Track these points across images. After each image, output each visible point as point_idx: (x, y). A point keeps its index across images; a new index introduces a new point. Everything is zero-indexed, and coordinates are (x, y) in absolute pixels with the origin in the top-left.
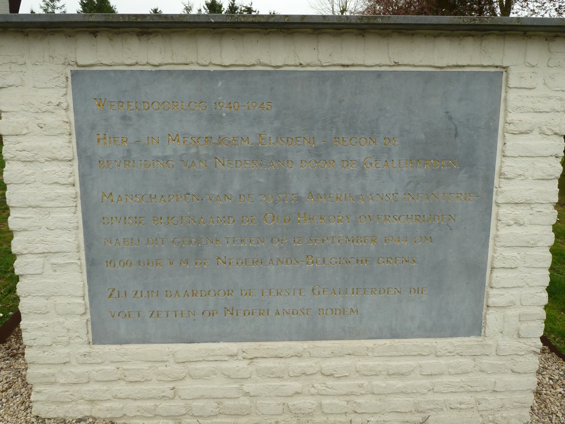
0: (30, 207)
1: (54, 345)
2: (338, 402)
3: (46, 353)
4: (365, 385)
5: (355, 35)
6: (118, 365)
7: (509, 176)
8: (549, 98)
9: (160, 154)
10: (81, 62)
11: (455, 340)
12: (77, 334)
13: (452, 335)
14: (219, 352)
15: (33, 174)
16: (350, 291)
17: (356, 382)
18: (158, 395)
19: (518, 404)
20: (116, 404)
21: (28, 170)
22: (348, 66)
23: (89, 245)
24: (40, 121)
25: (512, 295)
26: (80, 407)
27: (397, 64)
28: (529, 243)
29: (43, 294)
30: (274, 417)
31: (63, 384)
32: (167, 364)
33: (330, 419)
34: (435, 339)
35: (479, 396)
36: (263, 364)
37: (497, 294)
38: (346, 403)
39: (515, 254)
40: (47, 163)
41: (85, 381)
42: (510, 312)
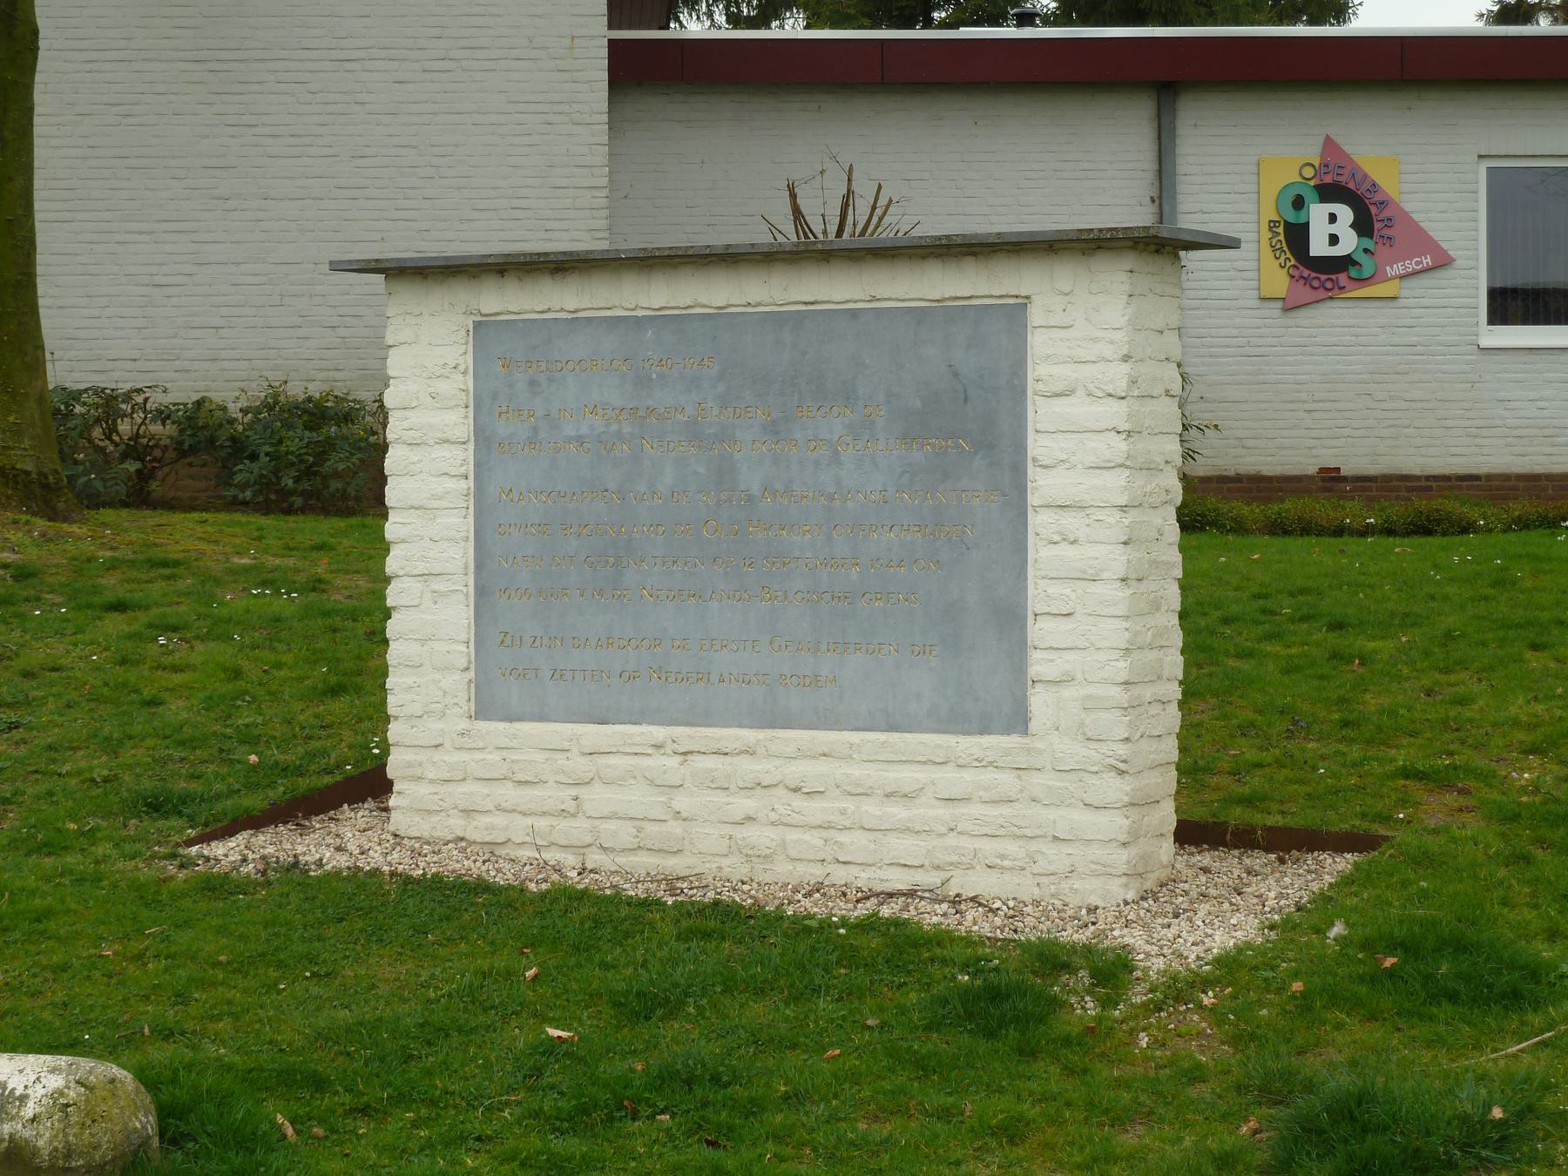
0: (413, 507)
1: (425, 717)
2: (809, 838)
3: (415, 729)
4: (849, 811)
5: (818, 261)
6: (505, 753)
7: (1044, 463)
8: (1095, 340)
9: (573, 433)
10: (484, 311)
11: (987, 740)
12: (456, 700)
13: (984, 730)
14: (638, 738)
15: (420, 461)
16: (824, 647)
17: (837, 805)
18: (554, 808)
19: (1099, 867)
20: (499, 820)
21: (414, 455)
22: (812, 303)
23: (480, 566)
24: (432, 390)
25: (1067, 661)
26: (452, 821)
27: (874, 299)
29: (418, 636)
30: (717, 859)
31: (432, 781)
32: (569, 754)
33: (798, 869)
34: (954, 736)
35: (1033, 846)
36: (700, 763)
37: (1043, 659)
38: (822, 842)
39: (1068, 591)
40: (437, 446)
41: (461, 777)
42: (1068, 692)
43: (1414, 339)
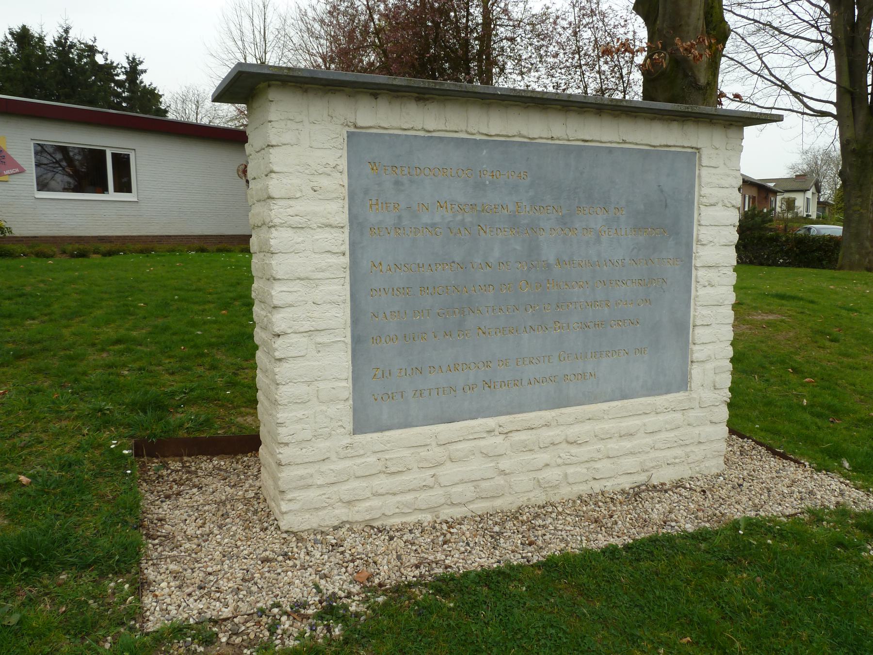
0: (299, 279)
3: (304, 450)
6: (379, 455)
7: (704, 243)
8: (728, 176)
9: (429, 221)
10: (360, 123)
12: (340, 423)
13: (668, 392)
15: (303, 242)
16: (589, 355)
20: (376, 502)
21: (298, 237)
23: (355, 320)
24: (315, 184)
26: (337, 512)
27: (624, 142)
28: (718, 301)
29: (306, 379)
32: (429, 448)
35: (688, 449)
36: (517, 437)
40: (319, 230)
43: (14, 194)
